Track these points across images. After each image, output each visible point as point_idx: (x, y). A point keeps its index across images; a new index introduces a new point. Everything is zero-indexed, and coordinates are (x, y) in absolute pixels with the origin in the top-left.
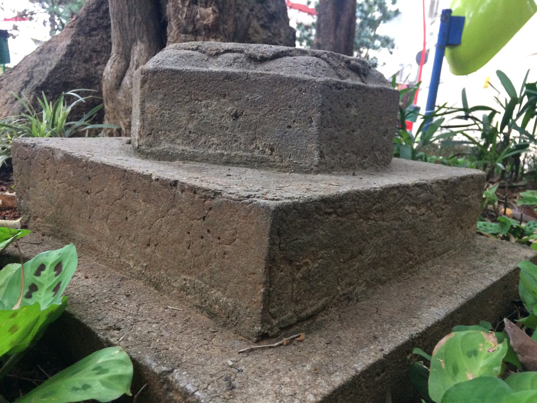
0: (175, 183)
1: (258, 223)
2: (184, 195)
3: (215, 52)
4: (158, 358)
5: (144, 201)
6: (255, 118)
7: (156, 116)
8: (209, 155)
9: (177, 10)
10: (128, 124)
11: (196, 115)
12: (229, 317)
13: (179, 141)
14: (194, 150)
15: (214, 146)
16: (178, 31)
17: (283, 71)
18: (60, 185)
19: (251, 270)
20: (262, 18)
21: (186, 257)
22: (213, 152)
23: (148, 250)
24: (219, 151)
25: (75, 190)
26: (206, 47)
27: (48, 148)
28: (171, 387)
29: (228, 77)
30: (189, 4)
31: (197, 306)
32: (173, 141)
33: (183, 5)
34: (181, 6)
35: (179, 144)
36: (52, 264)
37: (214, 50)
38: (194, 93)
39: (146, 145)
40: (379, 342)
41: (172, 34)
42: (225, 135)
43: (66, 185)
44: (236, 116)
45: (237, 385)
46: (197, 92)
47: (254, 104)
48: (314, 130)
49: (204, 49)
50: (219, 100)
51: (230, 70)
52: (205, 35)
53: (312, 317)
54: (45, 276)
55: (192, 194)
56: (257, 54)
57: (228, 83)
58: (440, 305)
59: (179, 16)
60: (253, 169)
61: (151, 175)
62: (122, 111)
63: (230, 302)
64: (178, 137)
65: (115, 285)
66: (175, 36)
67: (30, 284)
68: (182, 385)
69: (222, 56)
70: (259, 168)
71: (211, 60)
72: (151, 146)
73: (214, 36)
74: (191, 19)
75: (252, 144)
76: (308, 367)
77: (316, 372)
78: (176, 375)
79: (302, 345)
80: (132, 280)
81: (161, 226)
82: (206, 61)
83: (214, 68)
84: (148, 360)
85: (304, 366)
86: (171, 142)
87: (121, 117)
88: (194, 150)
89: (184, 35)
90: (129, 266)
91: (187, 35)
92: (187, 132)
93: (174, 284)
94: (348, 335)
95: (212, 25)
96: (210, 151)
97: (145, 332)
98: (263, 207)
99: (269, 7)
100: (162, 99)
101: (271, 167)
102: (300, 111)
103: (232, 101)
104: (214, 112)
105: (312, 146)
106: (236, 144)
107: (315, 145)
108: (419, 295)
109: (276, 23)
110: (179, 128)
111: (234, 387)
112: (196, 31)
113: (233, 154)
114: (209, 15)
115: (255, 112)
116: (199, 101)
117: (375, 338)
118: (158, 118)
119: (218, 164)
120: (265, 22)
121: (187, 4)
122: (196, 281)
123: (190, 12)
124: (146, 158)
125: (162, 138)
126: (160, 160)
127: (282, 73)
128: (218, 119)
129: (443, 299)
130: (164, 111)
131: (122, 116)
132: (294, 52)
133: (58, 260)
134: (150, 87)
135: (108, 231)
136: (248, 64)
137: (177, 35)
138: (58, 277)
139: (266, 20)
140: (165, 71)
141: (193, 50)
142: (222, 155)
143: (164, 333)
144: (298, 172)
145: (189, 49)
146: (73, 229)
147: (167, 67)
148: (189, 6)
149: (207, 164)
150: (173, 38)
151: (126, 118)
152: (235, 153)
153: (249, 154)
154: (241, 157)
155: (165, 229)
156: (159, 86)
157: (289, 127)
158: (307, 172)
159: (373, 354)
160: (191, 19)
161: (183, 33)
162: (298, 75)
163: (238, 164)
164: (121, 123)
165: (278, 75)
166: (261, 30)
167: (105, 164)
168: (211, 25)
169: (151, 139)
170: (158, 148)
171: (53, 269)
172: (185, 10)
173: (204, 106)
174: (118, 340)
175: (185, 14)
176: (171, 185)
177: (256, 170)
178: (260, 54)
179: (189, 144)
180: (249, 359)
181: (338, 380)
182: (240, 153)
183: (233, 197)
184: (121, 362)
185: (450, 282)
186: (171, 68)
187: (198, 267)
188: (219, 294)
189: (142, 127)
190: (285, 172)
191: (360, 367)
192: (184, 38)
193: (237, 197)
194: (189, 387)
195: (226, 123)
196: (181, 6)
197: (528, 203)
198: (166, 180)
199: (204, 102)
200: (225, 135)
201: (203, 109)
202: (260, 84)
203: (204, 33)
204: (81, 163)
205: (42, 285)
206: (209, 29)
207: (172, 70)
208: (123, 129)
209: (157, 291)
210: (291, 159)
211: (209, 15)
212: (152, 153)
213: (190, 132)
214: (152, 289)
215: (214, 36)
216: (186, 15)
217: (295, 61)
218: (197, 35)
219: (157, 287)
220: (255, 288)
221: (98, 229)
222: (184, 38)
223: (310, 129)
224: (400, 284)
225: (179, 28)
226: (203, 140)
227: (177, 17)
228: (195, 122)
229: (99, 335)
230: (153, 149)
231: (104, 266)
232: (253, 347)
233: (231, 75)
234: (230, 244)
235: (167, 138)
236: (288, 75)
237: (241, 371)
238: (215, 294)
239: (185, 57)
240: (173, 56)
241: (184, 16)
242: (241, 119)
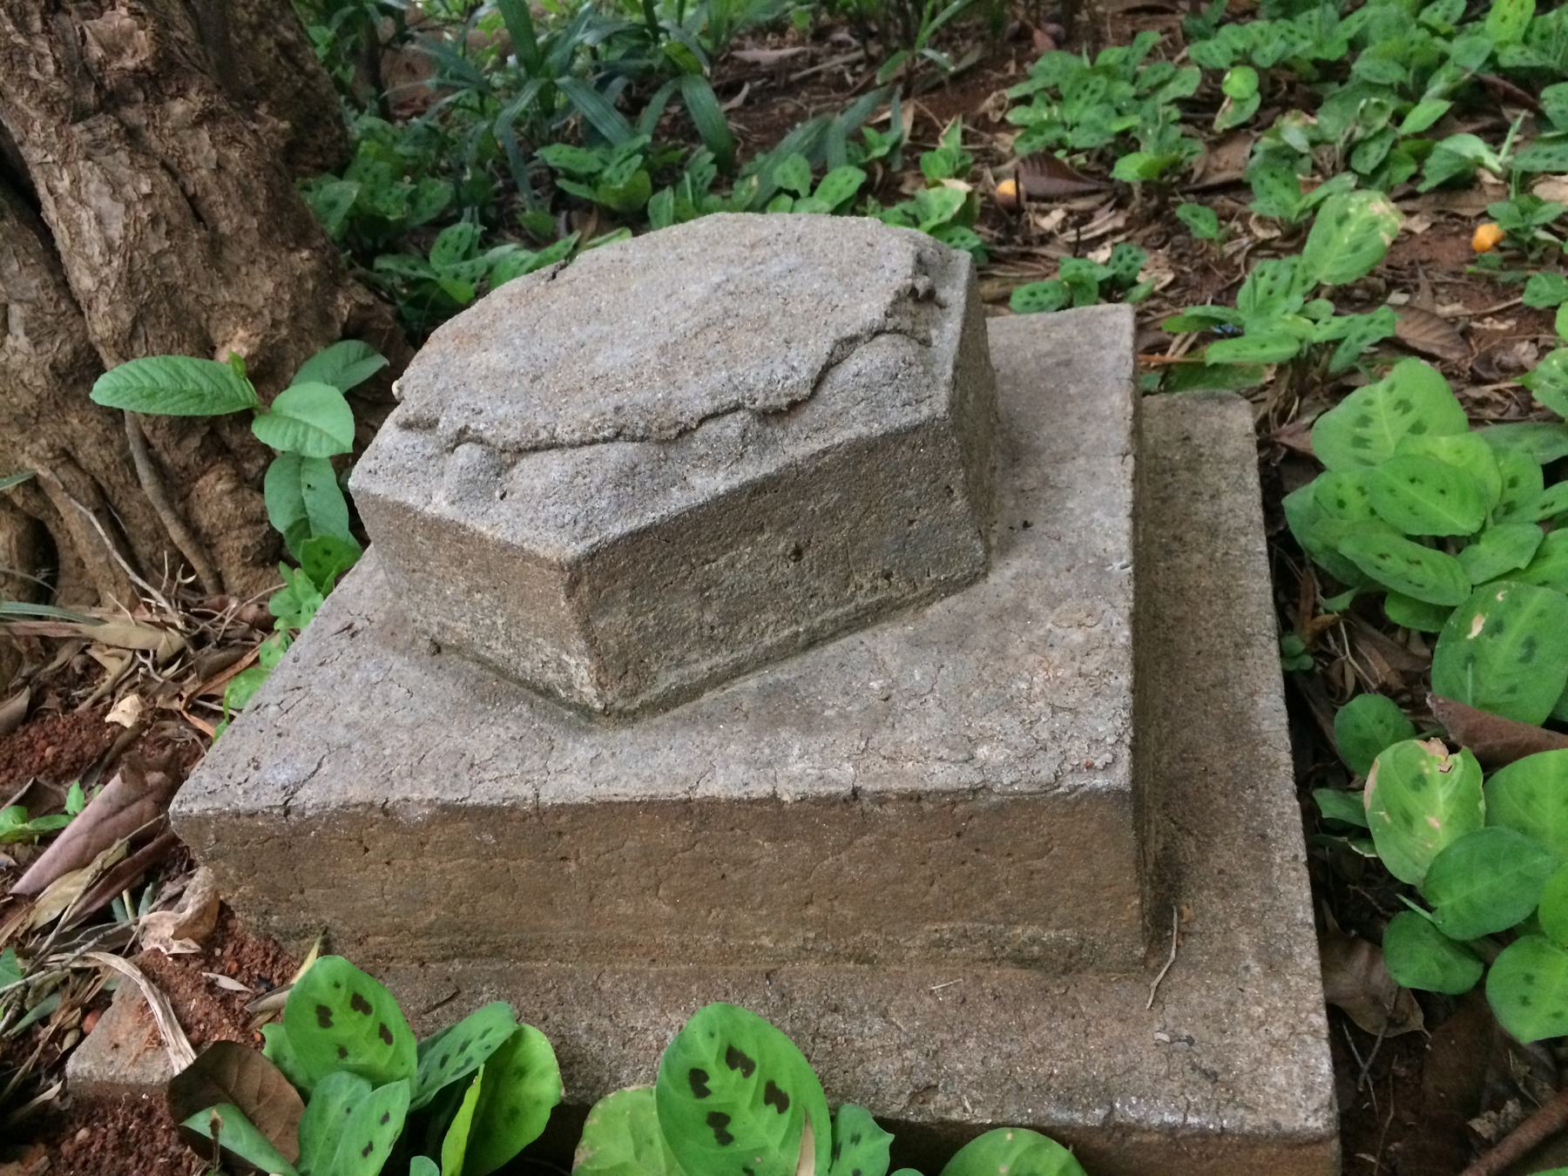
0: (856, 793)
1: (1102, 817)
2: (891, 811)
3: (673, 432)
4: (1068, 1102)
5: (769, 839)
6: (838, 539)
7: (628, 636)
8: (771, 649)
9: (16, 58)
10: (50, 455)
11: (714, 592)
12: (1071, 956)
13: (694, 656)
14: (735, 655)
15: (771, 628)
16: (54, 122)
17: (854, 419)
18: (449, 865)
19: (1105, 883)
21: (928, 898)
22: (775, 640)
23: (812, 911)
24: (786, 632)
25: (511, 864)
26: (642, 424)
27: (356, 806)
28: (1127, 1130)
29: (756, 489)
30: (45, 23)
31: (984, 960)
32: (680, 664)
33: (29, 36)
34: (21, 40)
35: (697, 661)
36: (717, 1062)
37: (669, 428)
38: (696, 554)
39: (625, 697)
40: (1275, 841)
41: (36, 134)
42: (788, 598)
43: (474, 861)
44: (798, 553)
45: (1217, 1068)
46: (702, 549)
47: (829, 513)
48: (959, 504)
49: (639, 433)
50: (753, 542)
51: (751, 471)
52: (146, 99)
54: (722, 1088)
55: (912, 805)
56: (778, 403)
57: (760, 501)
58: (1259, 683)
59: (34, 73)
60: (869, 632)
61: (775, 794)
62: (8, 425)
63: (1070, 936)
64: (689, 650)
65: (775, 998)
66: (54, 139)
67: (704, 1118)
68: (1156, 1121)
69: (698, 435)
70: (876, 621)
71: (672, 453)
72: (635, 694)
73: (173, 90)
74: (78, 67)
75: (847, 586)
76: (1256, 969)
77: (1273, 968)
78: (1130, 1111)
79: (1197, 927)
80: (785, 968)
81: (840, 869)
82: (666, 461)
83: (709, 483)
84: (1059, 1115)
85: (1247, 968)
86: (678, 666)
87: (14, 444)
88: (735, 655)
89: (81, 126)
90: (761, 947)
91: (91, 122)
92: (706, 632)
93: (909, 944)
94: (1223, 856)
95: (157, 61)
96: (767, 641)
97: (977, 1066)
98: (1108, 793)
100: (632, 599)
101: (899, 608)
102: (925, 485)
103: (781, 530)
104: (749, 567)
105: (966, 535)
106: (815, 601)
107: (971, 531)
108: (1210, 678)
110: (686, 630)
111: (1215, 1074)
112: (111, 95)
113: (817, 622)
114: (129, 35)
115: (835, 529)
116: (708, 562)
117: (1264, 837)
118: (634, 638)
119: (796, 654)
121: (37, 25)
122: (968, 926)
123: (61, 47)
124: (635, 720)
125: (654, 668)
126: (667, 710)
127: (865, 431)
128: (763, 576)
129: (1249, 663)
130: (640, 619)
131: (15, 439)
132: (837, 352)
133: (721, 1047)
134: (593, 589)
135: (667, 909)
136: (769, 430)
137: (59, 135)
138: (755, 1075)
140: (615, 543)
141: (605, 440)
142: (797, 634)
143: (1006, 1048)
144: (954, 592)
145: (593, 442)
146: (535, 930)
147: (616, 529)
148: (47, 30)
149: (771, 667)
150: (47, 146)
151: (33, 441)
152: (819, 619)
153: (850, 607)
154: (836, 620)
155: (851, 872)
156: (613, 577)
157: (911, 522)
158: (971, 584)
159: (1293, 874)
160: (77, 69)
161: (74, 122)
162: (901, 418)
163: (833, 636)
164: (28, 462)
165: (859, 438)
167: (610, 803)
168: (155, 64)
169: (630, 682)
170: (657, 691)
171: (727, 1068)
172: (42, 45)
173: (726, 566)
174: (965, 1110)
175: (50, 59)
176: (845, 800)
177: (876, 629)
178: (785, 401)
179: (717, 651)
180: (1171, 1009)
182: (830, 614)
183: (1025, 788)
184: (1037, 1148)
185: (1218, 607)
186: (626, 529)
187: (966, 906)
188: (1032, 930)
189: (602, 668)
190: (929, 604)
192: (88, 137)
193: (1035, 788)
194: (1168, 1118)
195: (783, 574)
196: (21, 40)
197: (1038, 142)
198: (829, 797)
199: (722, 561)
200: (788, 598)
201: (727, 573)
202: (829, 472)
203: (141, 96)
204: (516, 814)
205: (734, 1105)
206: (150, 77)
207: (631, 534)
208: (44, 473)
209: (866, 966)
210: (933, 576)
211: (129, 35)
212: (643, 706)
213: (712, 628)
214: (851, 965)
215: (173, 90)
216: (56, 61)
217: (863, 380)
218: (117, 107)
219: (860, 960)
220: (1120, 903)
221: (630, 911)
222: (88, 137)
223: (953, 506)
224: (1164, 667)
225: (51, 111)
226: (745, 629)
227: (25, 80)
228: (715, 606)
229: (913, 1119)
230: (642, 697)
231: (683, 967)
232: (1154, 984)
233: (763, 484)
234: (1040, 856)
235: (667, 663)
236: (877, 429)
237: (1190, 1041)
238: (1022, 932)
239: (624, 480)
240: (599, 491)
241: (51, 68)
242: (808, 556)
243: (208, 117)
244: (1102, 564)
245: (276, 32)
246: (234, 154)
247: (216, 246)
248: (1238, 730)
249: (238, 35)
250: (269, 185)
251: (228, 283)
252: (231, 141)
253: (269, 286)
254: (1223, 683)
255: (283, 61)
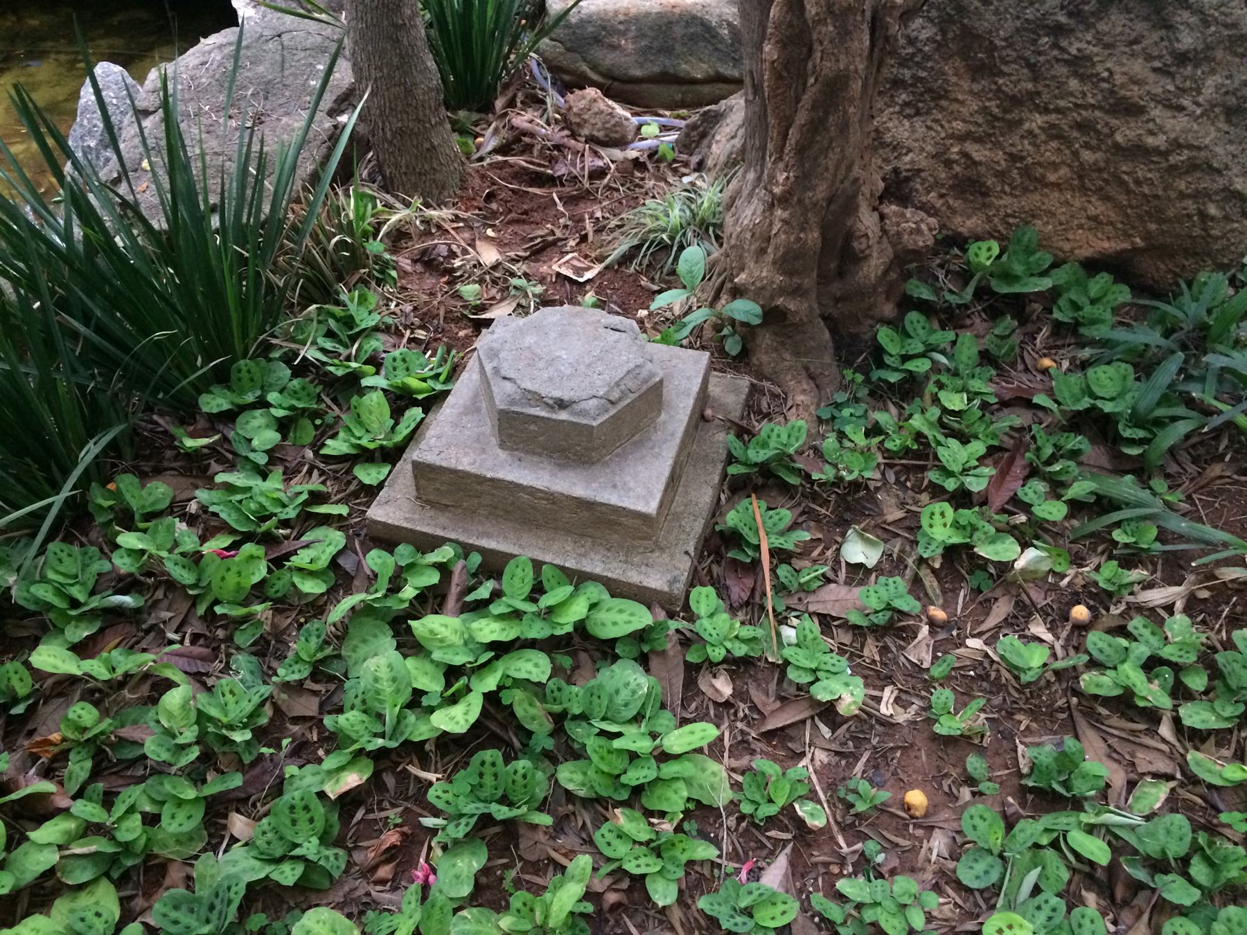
20: (1160, 57)
53: (447, 506)
99: (1178, 40)
109: (1196, 67)
120: (1165, 65)
139: (1169, 60)
166: (1152, 77)
181: (405, 525)
191: (418, 528)
243: (785, 222)
244: (492, 470)
245: (1204, 204)
246: (783, 237)
247: (762, 251)
248: (488, 535)
249: (1165, 190)
250: (785, 253)
251: (756, 262)
252: (786, 233)
253: (764, 274)
254: (506, 537)
255: (1195, 218)
